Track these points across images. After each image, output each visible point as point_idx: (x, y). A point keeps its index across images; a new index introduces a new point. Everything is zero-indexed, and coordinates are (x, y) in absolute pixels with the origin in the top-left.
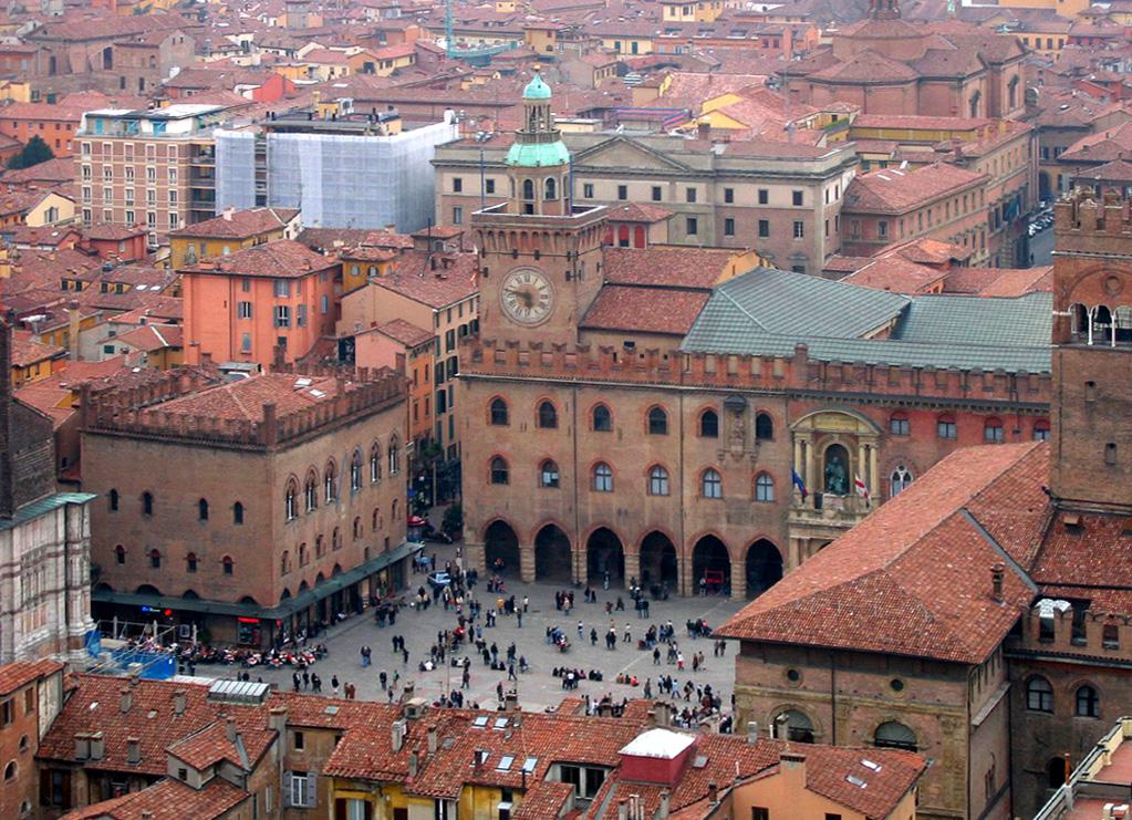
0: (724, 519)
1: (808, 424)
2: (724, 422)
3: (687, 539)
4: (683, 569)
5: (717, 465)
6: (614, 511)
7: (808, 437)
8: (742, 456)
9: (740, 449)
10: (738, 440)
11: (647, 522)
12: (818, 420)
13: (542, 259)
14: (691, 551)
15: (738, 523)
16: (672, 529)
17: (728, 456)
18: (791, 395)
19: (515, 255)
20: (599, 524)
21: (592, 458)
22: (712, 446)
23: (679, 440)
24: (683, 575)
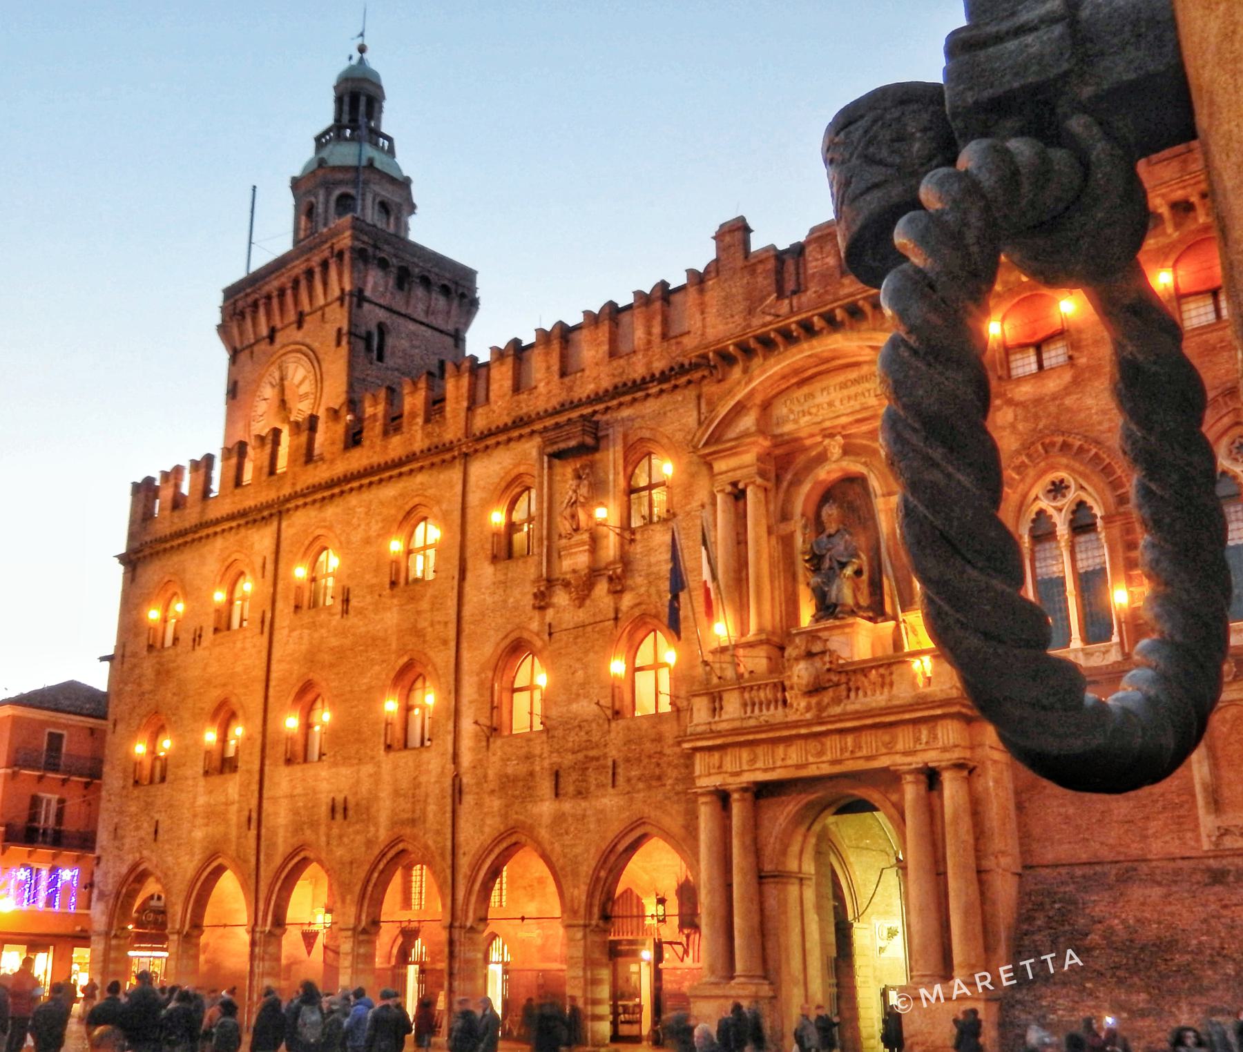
6: (324, 810)
12: (781, 410)
15: (581, 794)
19: (271, 337)
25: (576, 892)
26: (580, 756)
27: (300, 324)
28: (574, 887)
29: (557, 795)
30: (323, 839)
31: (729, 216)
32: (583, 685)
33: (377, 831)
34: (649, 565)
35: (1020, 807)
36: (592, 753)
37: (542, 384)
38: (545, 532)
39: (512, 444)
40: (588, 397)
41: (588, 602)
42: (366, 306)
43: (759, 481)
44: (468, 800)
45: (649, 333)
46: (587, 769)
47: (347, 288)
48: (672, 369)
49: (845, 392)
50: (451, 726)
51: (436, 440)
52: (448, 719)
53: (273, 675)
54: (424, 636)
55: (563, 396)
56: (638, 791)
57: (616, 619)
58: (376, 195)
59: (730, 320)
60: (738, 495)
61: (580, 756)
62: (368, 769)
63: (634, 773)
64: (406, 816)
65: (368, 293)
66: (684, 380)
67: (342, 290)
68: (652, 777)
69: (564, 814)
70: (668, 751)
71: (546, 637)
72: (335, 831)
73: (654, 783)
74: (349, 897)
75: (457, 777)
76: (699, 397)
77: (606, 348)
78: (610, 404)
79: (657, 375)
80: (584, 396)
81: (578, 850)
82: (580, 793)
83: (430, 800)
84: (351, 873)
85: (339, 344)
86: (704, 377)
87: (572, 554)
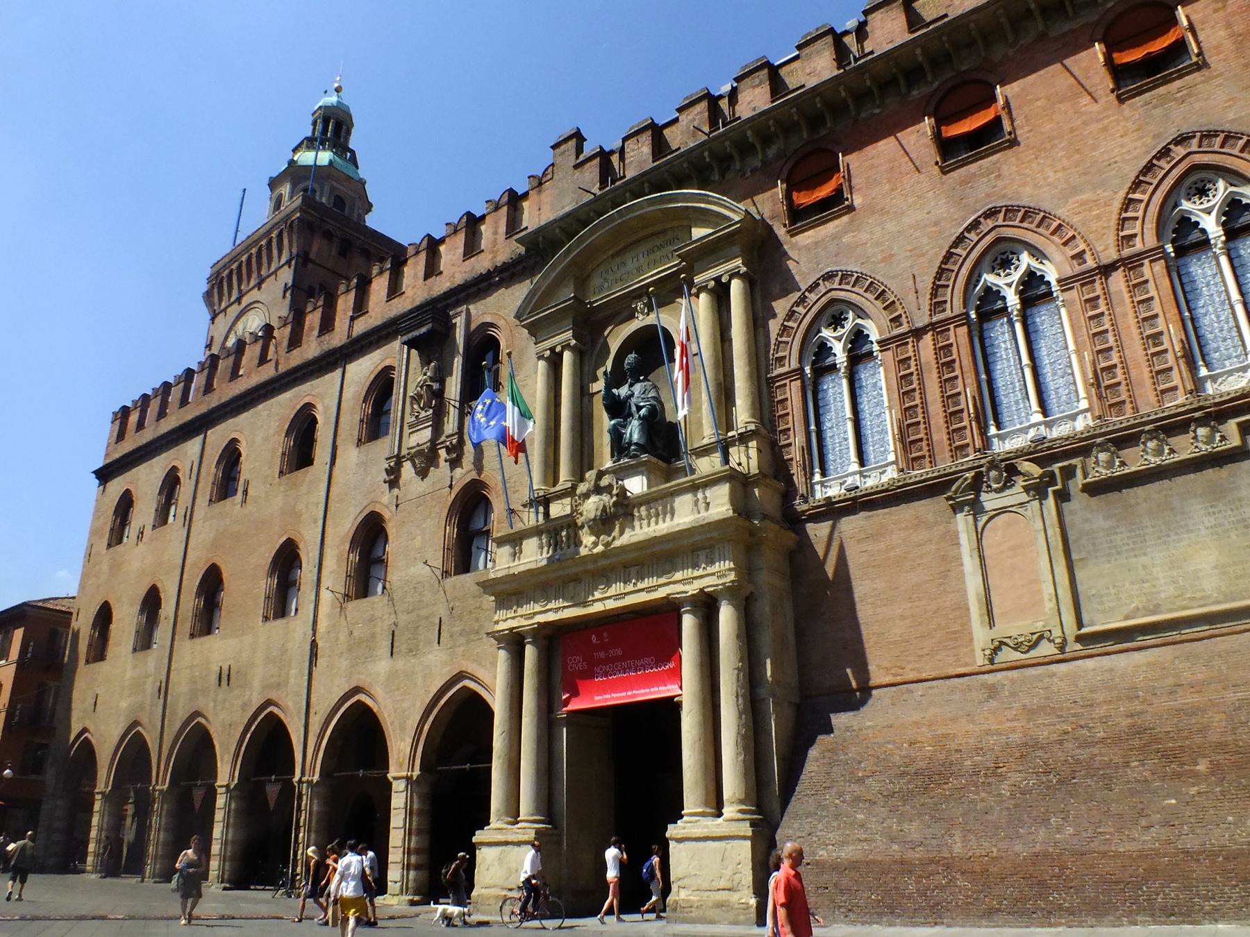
5: (384, 501)
6: (214, 677)
13: (263, 286)
15: (413, 651)
19: (239, 300)
27: (259, 286)
30: (212, 704)
35: (800, 634)
36: (424, 612)
42: (310, 266)
44: (322, 661)
45: (496, 233)
47: (294, 251)
49: (652, 257)
50: (313, 597)
53: (188, 562)
58: (333, 189)
60: (555, 362)
62: (248, 639)
64: (273, 680)
65: (312, 256)
72: (220, 697)
73: (473, 637)
75: (314, 644)
77: (461, 250)
81: (406, 705)
82: (411, 651)
85: (284, 297)
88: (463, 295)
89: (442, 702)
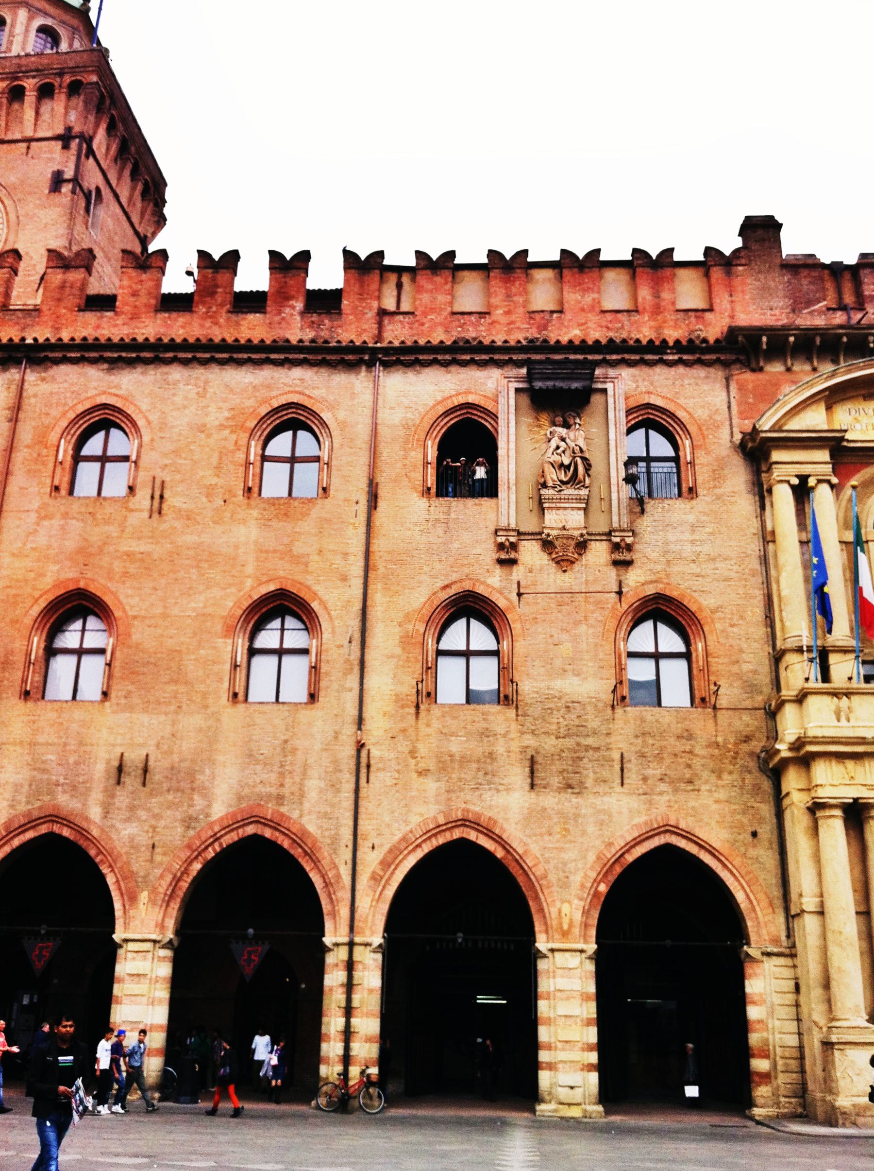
0: (518, 776)
1: (815, 419)
2: (522, 446)
3: (370, 860)
4: (349, 986)
5: (494, 584)
7: (818, 461)
8: (582, 546)
9: (574, 520)
10: (569, 491)
11: (220, 802)
14: (385, 907)
16: (312, 826)
17: (530, 553)
18: (742, 350)
20: (31, 823)
21: (48, 581)
22: (475, 522)
23: (363, 507)
24: (349, 1011)
25: (566, 909)
26: (570, 742)
28: (563, 902)
29: (532, 786)
31: (760, 210)
32: (572, 661)
33: (209, 806)
34: (666, 543)
36: (590, 741)
37: (500, 311)
38: (513, 477)
39: (454, 369)
40: (570, 341)
41: (577, 567)
43: (835, 480)
46: (581, 759)
48: (691, 341)
51: (324, 334)
52: (348, 671)
54: (306, 565)
55: (533, 333)
56: (661, 793)
57: (620, 593)
59: (769, 312)
60: (802, 492)
61: (570, 742)
63: (654, 771)
65: (95, 147)
66: (714, 357)
67: (69, 129)
68: (681, 780)
69: (544, 809)
70: (698, 750)
71: (514, 598)
74: (144, 896)
76: (727, 380)
78: (608, 357)
79: (671, 344)
80: (564, 340)
82: (570, 787)
83: (313, 773)
84: (151, 860)
86: (737, 361)
87: (558, 508)
88: (614, 357)
89: (630, 858)
